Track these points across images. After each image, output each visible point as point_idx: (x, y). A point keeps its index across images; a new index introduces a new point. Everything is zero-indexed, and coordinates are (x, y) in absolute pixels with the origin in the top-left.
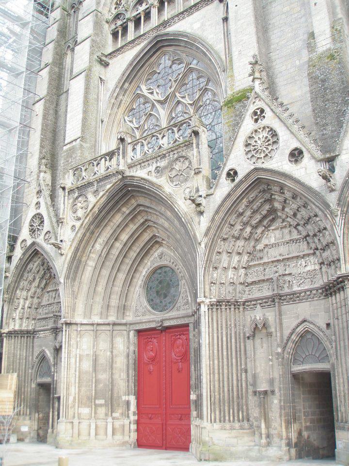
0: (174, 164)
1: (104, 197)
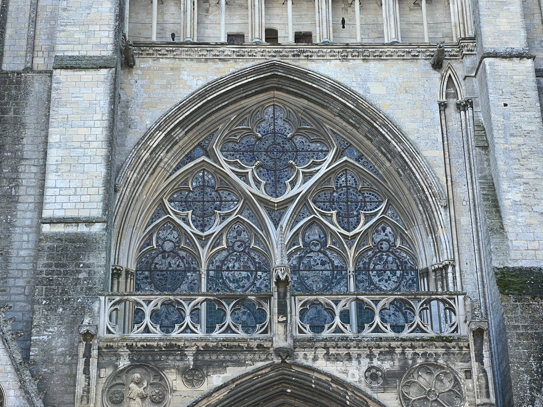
0: (416, 375)
1: (223, 390)
